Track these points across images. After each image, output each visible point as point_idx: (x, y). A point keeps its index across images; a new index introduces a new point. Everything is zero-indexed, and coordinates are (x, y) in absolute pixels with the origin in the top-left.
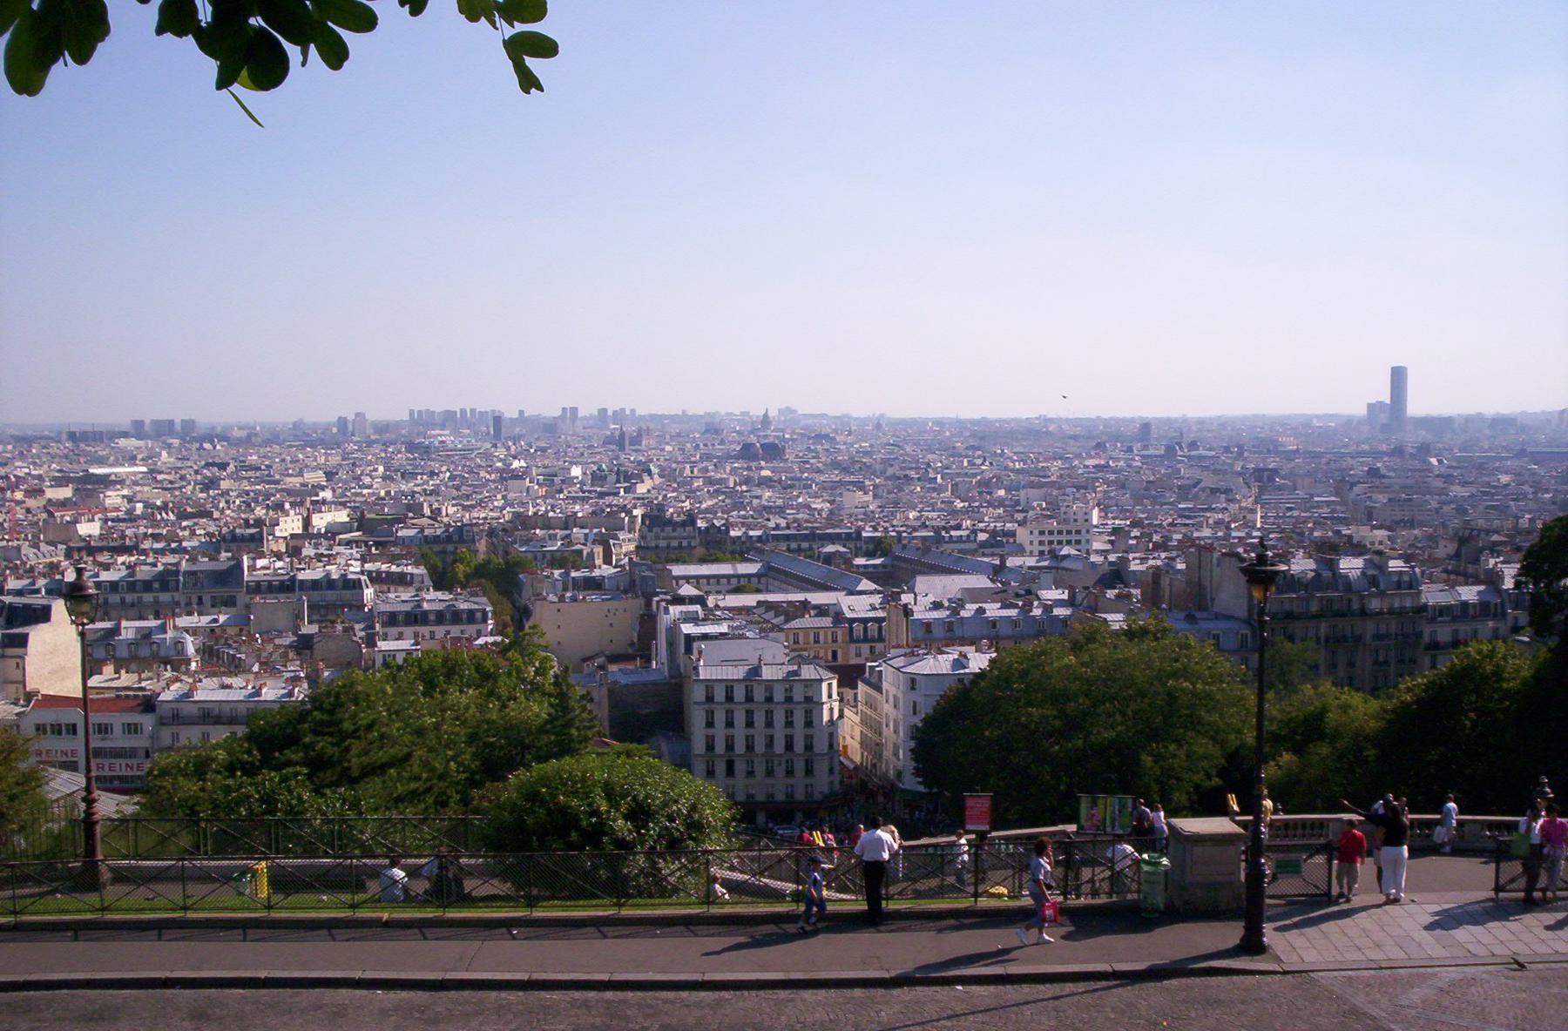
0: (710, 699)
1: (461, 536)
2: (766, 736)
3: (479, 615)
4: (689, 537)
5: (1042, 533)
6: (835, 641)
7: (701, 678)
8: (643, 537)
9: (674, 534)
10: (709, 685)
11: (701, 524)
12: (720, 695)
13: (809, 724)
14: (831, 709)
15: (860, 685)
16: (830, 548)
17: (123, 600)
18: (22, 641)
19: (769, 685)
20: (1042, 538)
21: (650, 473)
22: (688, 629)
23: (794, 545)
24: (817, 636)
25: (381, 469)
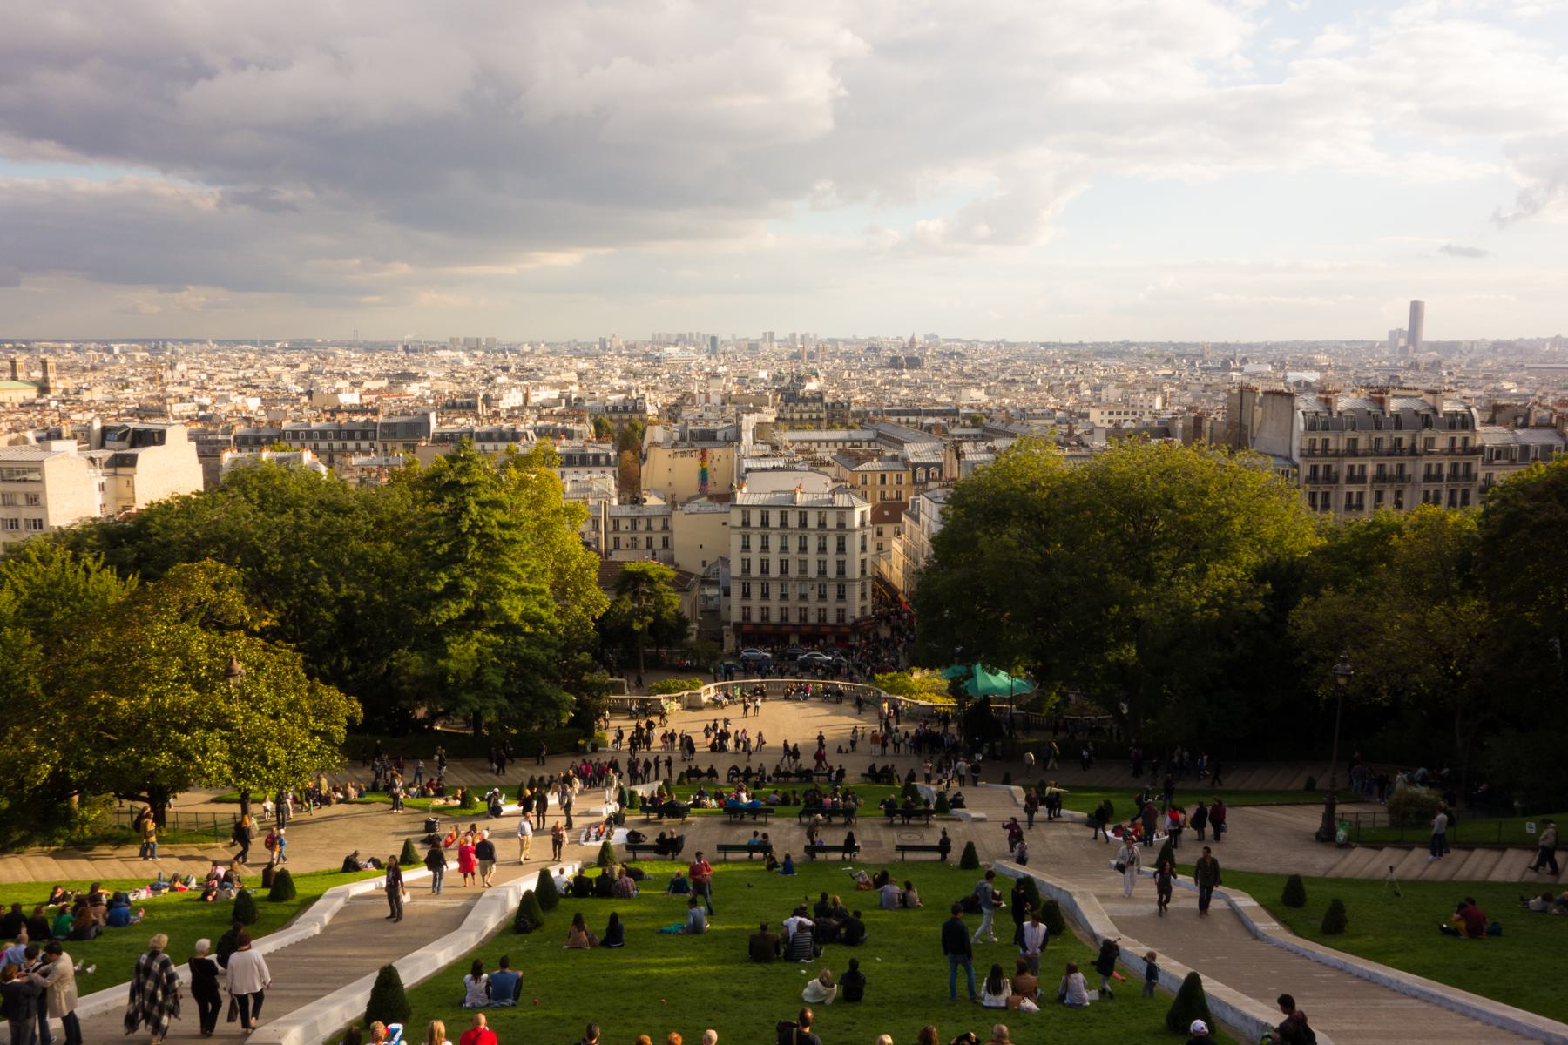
0: (746, 524)
1: (635, 407)
2: (800, 561)
3: (603, 459)
4: (818, 411)
5: (1111, 413)
6: (899, 483)
7: (738, 503)
8: (781, 411)
9: (807, 409)
10: (746, 510)
11: (827, 400)
12: (756, 520)
13: (841, 549)
14: (864, 537)
15: (904, 518)
16: (930, 420)
17: (331, 447)
18: (131, 461)
19: (803, 514)
20: (1111, 417)
21: (817, 375)
22: (747, 464)
23: (903, 419)
24: (883, 478)
25: (619, 372)
